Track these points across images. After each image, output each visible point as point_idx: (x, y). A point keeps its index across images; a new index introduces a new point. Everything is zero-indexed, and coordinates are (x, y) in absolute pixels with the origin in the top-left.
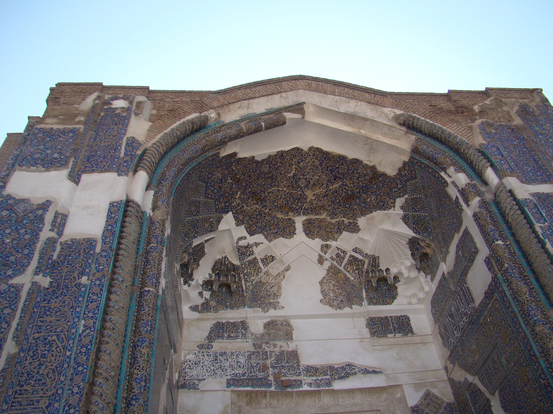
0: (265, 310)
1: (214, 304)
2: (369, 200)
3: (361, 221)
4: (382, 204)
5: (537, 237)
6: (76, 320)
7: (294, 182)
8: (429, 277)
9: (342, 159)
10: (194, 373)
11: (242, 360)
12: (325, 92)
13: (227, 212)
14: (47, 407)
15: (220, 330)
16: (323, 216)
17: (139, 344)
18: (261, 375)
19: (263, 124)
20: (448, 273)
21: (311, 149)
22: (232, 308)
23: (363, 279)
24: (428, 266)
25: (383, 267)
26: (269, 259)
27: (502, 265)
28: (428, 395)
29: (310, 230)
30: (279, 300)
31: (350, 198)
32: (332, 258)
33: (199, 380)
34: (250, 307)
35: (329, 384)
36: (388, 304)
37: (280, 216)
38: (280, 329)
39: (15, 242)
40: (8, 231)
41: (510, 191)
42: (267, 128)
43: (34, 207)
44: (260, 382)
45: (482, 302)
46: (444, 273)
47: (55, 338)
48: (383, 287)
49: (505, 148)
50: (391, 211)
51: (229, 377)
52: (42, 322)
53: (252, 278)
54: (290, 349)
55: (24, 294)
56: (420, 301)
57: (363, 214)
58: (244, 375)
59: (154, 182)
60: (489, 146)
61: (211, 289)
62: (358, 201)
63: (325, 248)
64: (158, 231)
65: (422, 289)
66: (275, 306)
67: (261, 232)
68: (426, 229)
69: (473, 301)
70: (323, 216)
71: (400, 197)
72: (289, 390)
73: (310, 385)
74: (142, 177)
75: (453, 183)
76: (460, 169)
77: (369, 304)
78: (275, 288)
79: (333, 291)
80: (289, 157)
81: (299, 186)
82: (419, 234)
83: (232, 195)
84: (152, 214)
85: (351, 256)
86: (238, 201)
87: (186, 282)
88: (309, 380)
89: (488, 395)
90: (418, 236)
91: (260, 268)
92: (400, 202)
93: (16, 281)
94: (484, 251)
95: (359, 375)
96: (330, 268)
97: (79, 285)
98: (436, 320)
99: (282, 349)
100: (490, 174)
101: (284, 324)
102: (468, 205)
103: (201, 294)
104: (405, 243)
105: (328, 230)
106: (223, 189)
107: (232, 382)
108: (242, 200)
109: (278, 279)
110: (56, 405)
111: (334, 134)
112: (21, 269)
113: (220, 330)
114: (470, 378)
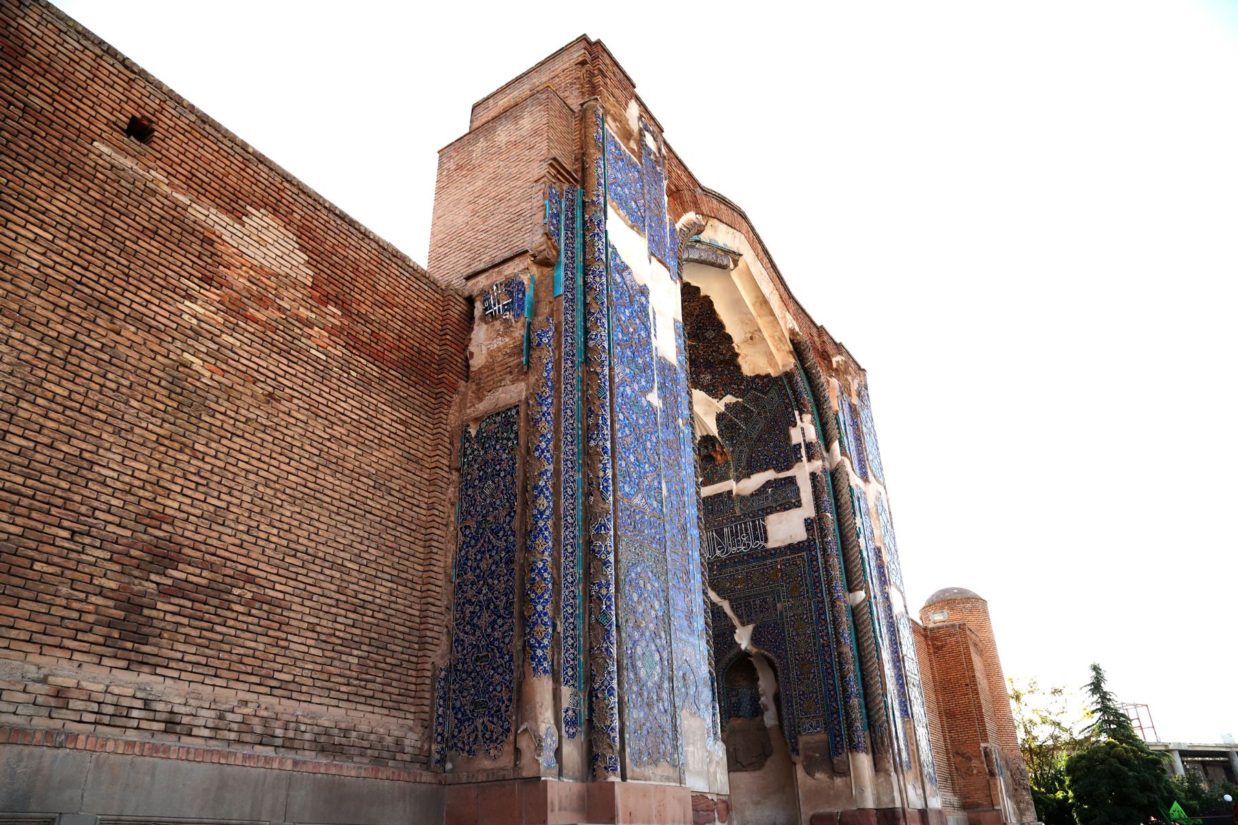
9: (721, 326)
20: (737, 495)
21: (707, 297)
27: (826, 536)
45: (779, 548)
46: (730, 492)
50: (714, 401)
68: (732, 439)
69: (766, 540)
75: (802, 429)
76: (812, 422)
89: (736, 622)
92: (729, 399)
94: (808, 509)
100: (836, 446)
102: (809, 460)
111: (738, 302)
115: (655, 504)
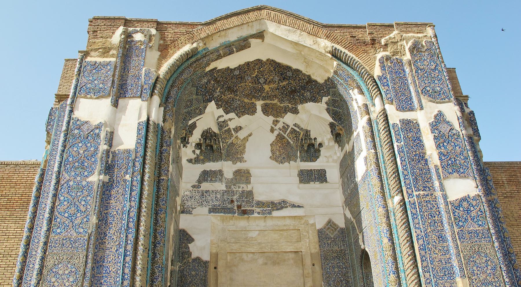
0: (235, 163)
1: (202, 158)
2: (305, 95)
3: (300, 107)
4: (314, 98)
5: (394, 151)
6: (126, 202)
7: (256, 80)
8: (340, 148)
9: (289, 68)
10: (190, 203)
11: (219, 196)
12: (279, 23)
13: (211, 101)
14: (116, 251)
15: (205, 176)
16: (276, 101)
17: (159, 212)
18: (229, 206)
19: (235, 49)
21: (268, 60)
22: (214, 161)
23: (299, 144)
24: (340, 141)
25: (312, 137)
26: (238, 129)
28: (330, 222)
29: (266, 110)
30: (244, 156)
31: (293, 92)
32: (280, 129)
33: (193, 208)
34: (225, 160)
35: (270, 213)
36: (313, 161)
37: (246, 100)
38: (243, 176)
39: (86, 153)
40: (80, 145)
41: (387, 115)
42: (237, 51)
43: (93, 127)
44: (229, 211)
47: (115, 213)
48: (312, 150)
49: (393, 80)
51: (210, 207)
52: (108, 203)
53: (227, 141)
54: (248, 190)
55: (95, 187)
56: (334, 161)
57: (302, 103)
58: (219, 206)
59: (164, 99)
60: (382, 78)
61: (200, 148)
62: (298, 94)
63: (276, 122)
64: (167, 138)
65: (336, 153)
66: (241, 160)
67: (234, 111)
70: (276, 101)
71: (325, 96)
72: (246, 216)
73: (259, 213)
74: (156, 99)
75: (356, 100)
76: (362, 92)
77: (301, 161)
78: (242, 148)
79: (279, 151)
80: (253, 65)
81: (260, 82)
82: (336, 121)
83: (214, 91)
84: (163, 125)
85: (292, 128)
86: (218, 94)
87: (184, 146)
88: (258, 210)
90: (335, 122)
91: (232, 134)
92: (325, 99)
93: (90, 179)
95: (289, 208)
96: (278, 135)
97: (125, 181)
98: (342, 176)
99: (244, 189)
101: (246, 172)
103: (194, 152)
104: (327, 124)
105: (278, 110)
106: (208, 88)
107: (212, 210)
108: (221, 93)
109: (244, 141)
110: (121, 250)
111: (284, 52)
112: (91, 173)
113: (205, 176)
114: (352, 219)
115: (82, 230)
